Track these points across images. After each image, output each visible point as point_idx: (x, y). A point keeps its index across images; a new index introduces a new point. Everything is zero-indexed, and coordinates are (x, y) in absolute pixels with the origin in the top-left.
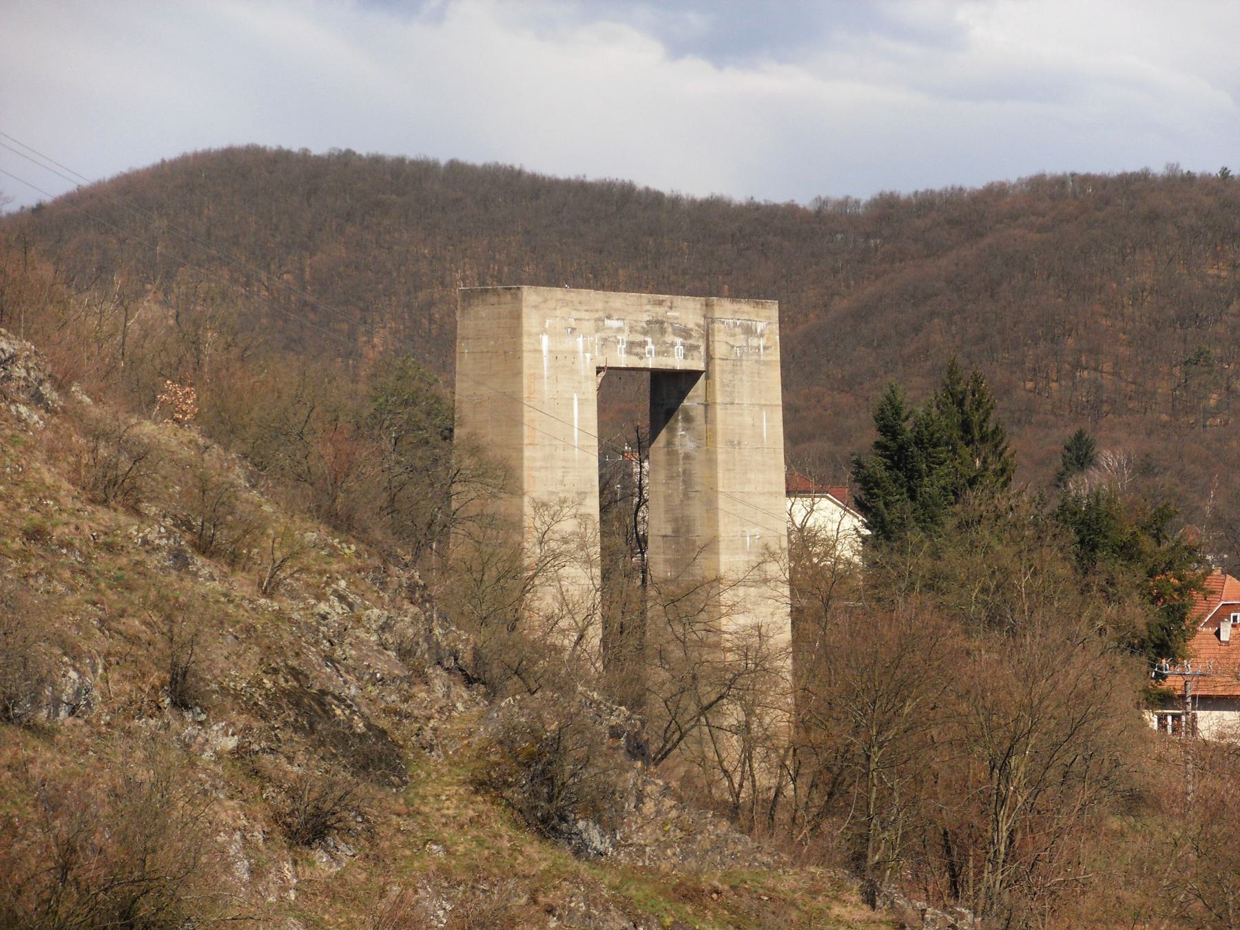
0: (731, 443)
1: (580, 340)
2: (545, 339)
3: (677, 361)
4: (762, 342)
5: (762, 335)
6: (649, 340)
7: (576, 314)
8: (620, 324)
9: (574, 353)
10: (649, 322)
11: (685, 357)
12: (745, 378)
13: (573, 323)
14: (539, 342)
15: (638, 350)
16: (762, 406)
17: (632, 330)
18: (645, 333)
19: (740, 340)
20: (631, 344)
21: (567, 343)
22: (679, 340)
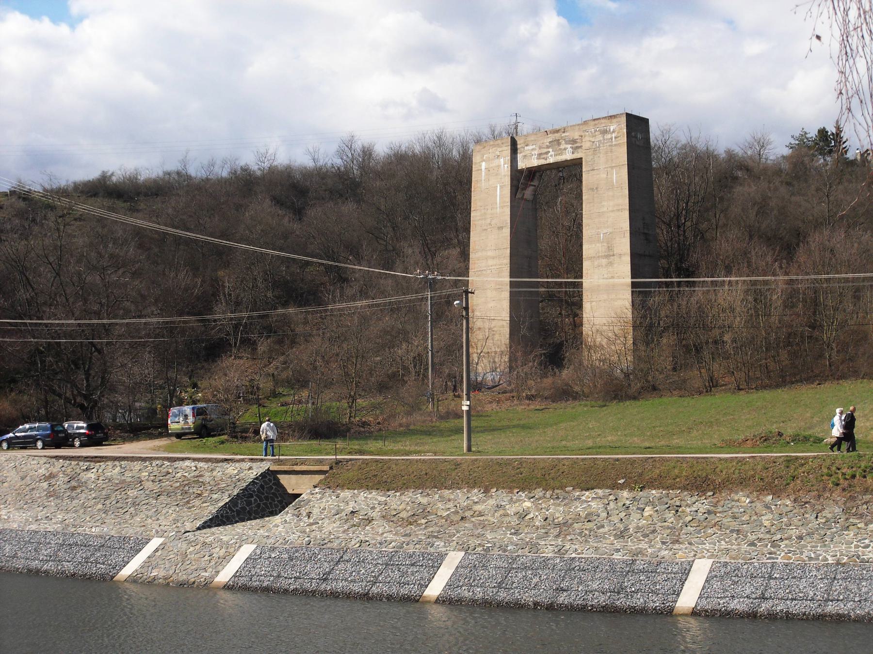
0: (592, 189)
1: (502, 160)
2: (483, 164)
3: (568, 156)
4: (614, 135)
5: (614, 132)
6: (551, 150)
7: (499, 149)
8: (534, 147)
9: (499, 166)
10: (550, 142)
11: (573, 153)
12: (601, 155)
13: (498, 153)
14: (481, 166)
15: (545, 156)
16: (612, 167)
17: (540, 148)
18: (548, 147)
19: (600, 137)
20: (540, 154)
21: (496, 162)
22: (569, 146)
